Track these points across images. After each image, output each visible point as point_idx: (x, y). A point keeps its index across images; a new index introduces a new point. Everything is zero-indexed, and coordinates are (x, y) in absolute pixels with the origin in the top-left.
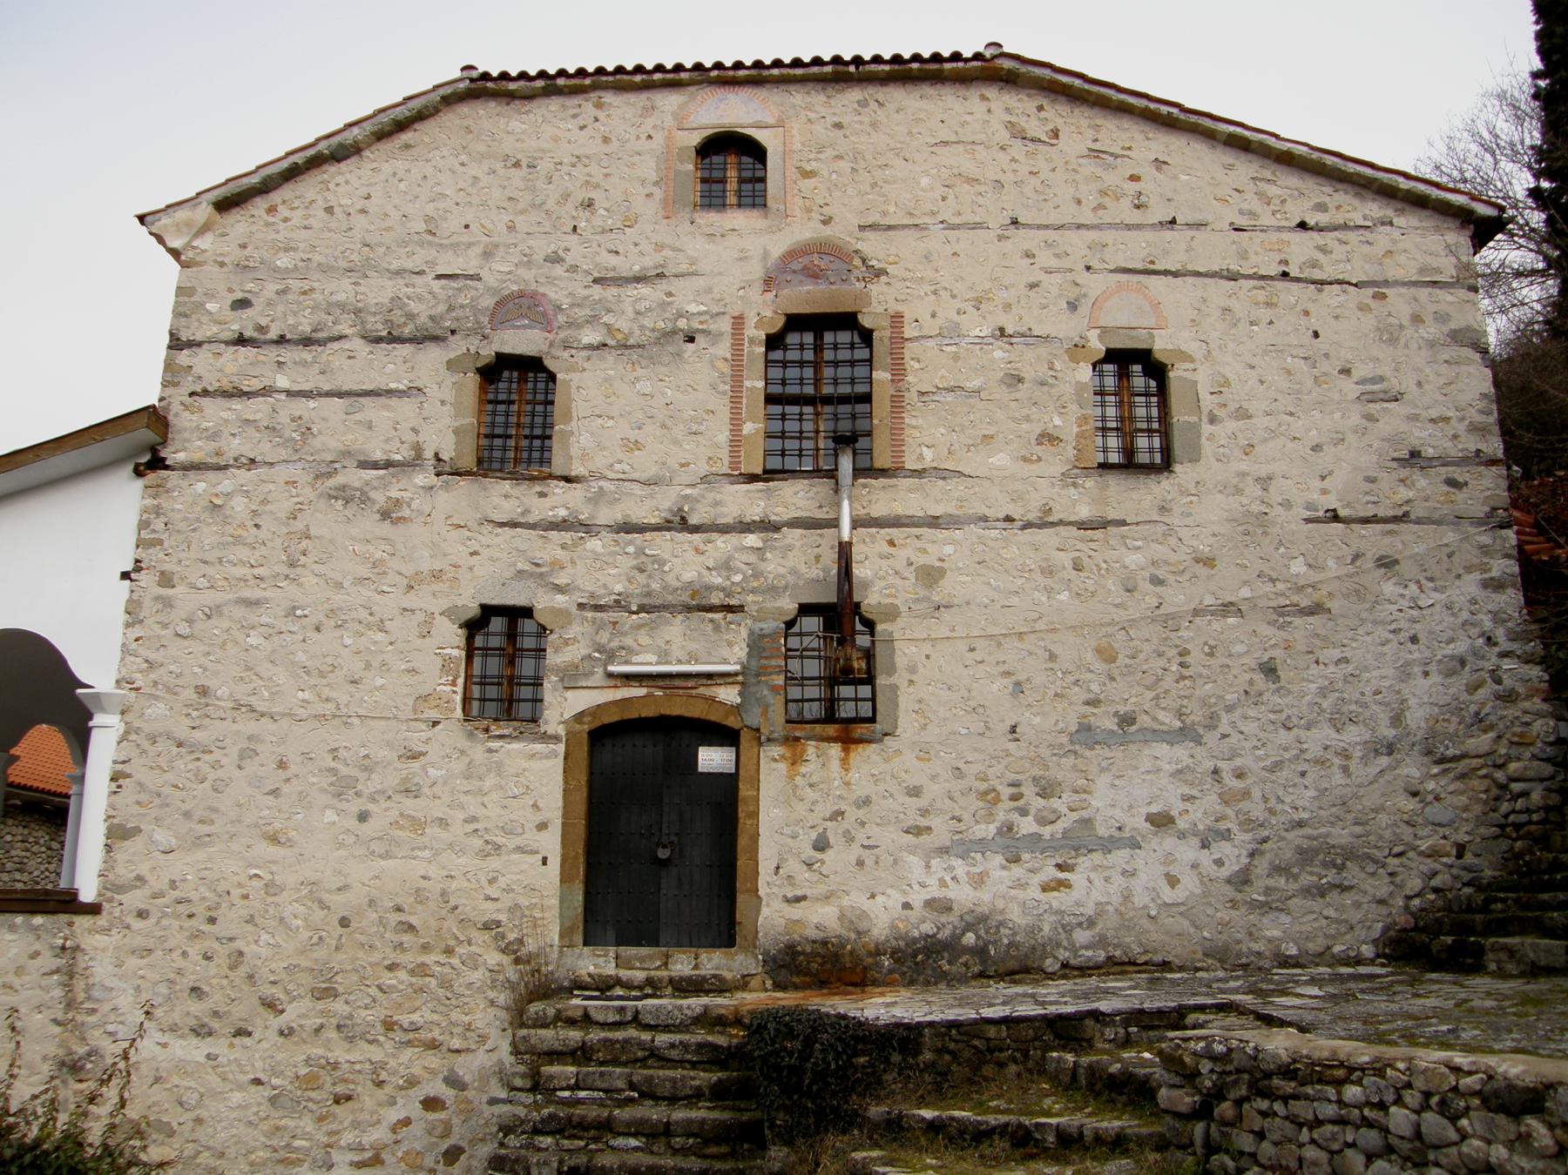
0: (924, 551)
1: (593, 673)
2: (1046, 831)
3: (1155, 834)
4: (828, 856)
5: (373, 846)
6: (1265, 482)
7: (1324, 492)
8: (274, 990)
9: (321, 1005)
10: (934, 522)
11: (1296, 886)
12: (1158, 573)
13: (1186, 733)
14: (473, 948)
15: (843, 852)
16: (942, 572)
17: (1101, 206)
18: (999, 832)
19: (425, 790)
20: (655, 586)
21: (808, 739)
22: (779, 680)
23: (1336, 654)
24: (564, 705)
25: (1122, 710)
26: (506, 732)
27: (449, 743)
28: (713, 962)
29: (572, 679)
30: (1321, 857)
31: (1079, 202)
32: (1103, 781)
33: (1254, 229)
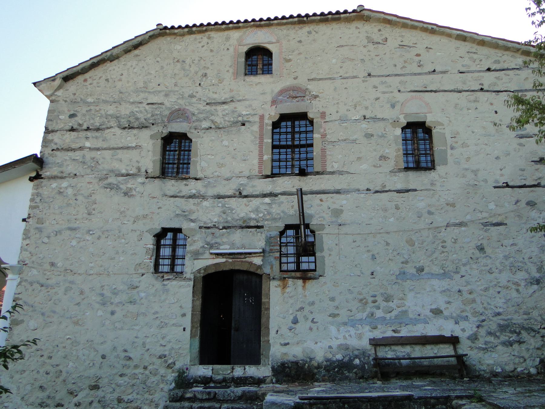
0: (334, 203)
1: (204, 253)
2: (388, 316)
3: (435, 318)
4: (297, 326)
5: (117, 324)
6: (475, 172)
7: (502, 175)
8: (74, 386)
9: (92, 392)
10: (338, 192)
11: (499, 341)
12: (431, 210)
13: (445, 275)
14: (154, 367)
15: (303, 325)
16: (342, 211)
17: (404, 67)
18: (367, 316)
19: (138, 301)
20: (229, 219)
21: (289, 278)
22: (278, 255)
23: (511, 241)
24: (194, 265)
25: (418, 265)
26: (170, 277)
27: (149, 280)
28: (252, 371)
29: (197, 255)
30: (509, 328)
31: (395, 66)
32: (410, 295)
33: (468, 72)
